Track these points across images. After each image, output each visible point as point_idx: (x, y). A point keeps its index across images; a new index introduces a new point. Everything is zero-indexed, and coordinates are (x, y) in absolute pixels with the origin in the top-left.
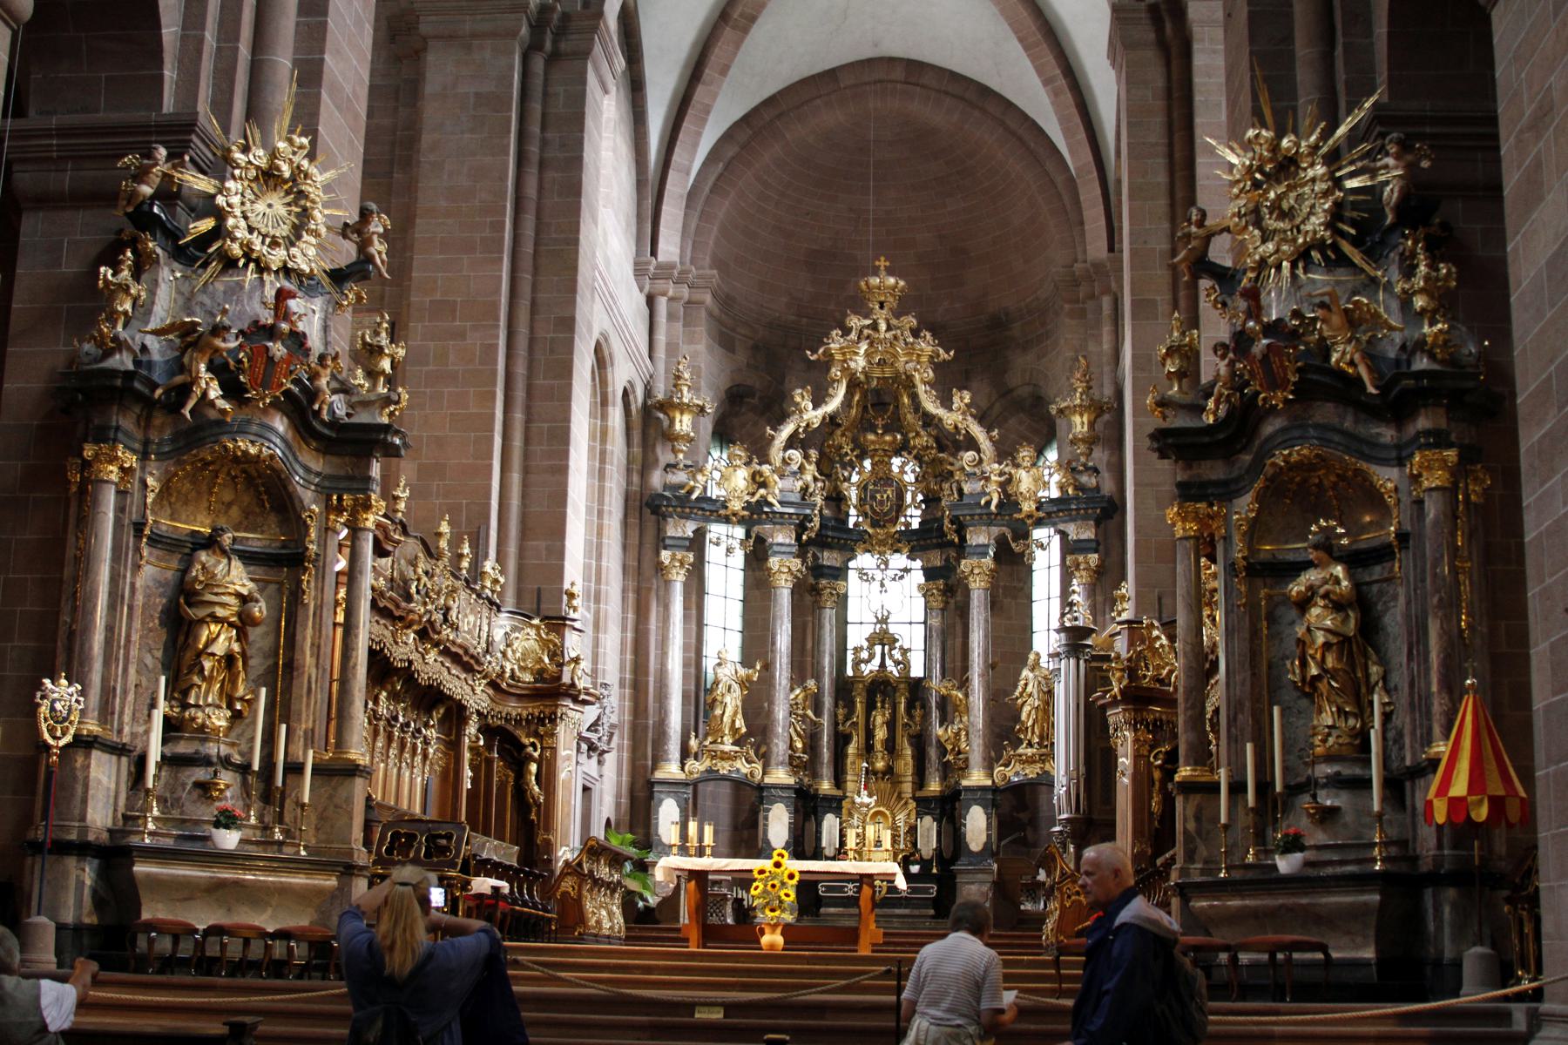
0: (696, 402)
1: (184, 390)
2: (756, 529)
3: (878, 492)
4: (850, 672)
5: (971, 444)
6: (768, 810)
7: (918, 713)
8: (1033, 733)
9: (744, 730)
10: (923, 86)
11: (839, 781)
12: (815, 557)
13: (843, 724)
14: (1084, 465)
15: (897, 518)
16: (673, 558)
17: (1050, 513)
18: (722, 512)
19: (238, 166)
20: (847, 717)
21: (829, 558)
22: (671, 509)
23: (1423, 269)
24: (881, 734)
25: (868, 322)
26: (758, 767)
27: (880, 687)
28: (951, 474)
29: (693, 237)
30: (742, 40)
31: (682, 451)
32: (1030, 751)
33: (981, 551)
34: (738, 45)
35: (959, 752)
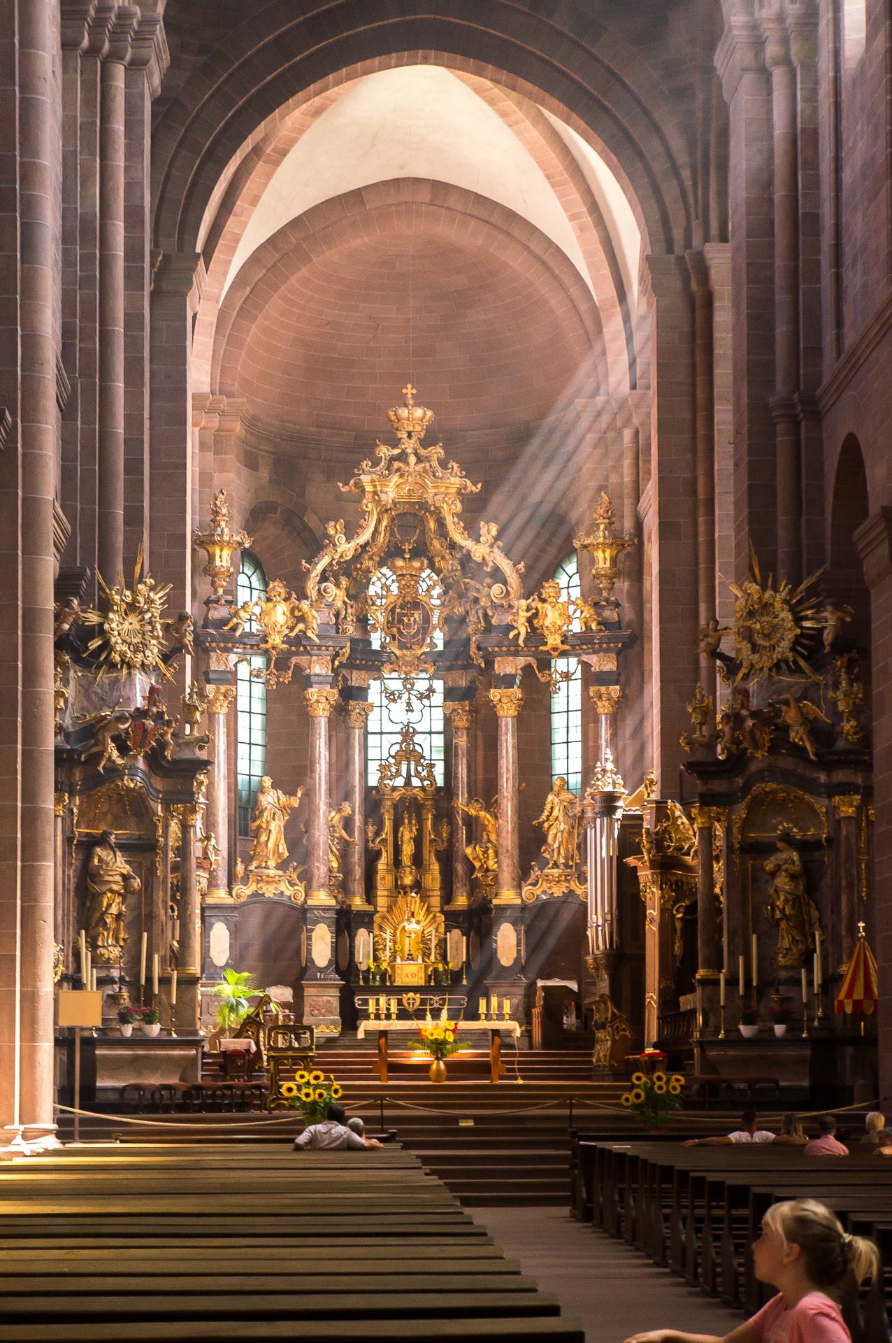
0: (235, 538)
1: (98, 756)
2: (294, 660)
3: (405, 615)
5: (497, 575)
6: (312, 930)
8: (559, 854)
9: (286, 854)
10: (448, 208)
11: (370, 896)
13: (373, 842)
14: (607, 600)
15: (424, 640)
17: (574, 645)
18: (263, 646)
19: (117, 604)
20: (377, 834)
21: (356, 679)
22: (214, 644)
23: (844, 683)
24: (408, 849)
25: (396, 452)
26: (301, 888)
27: (409, 807)
28: (476, 600)
29: (222, 364)
30: (272, 173)
31: (222, 586)
32: (556, 871)
33: (508, 681)
34: (269, 176)
35: (487, 870)
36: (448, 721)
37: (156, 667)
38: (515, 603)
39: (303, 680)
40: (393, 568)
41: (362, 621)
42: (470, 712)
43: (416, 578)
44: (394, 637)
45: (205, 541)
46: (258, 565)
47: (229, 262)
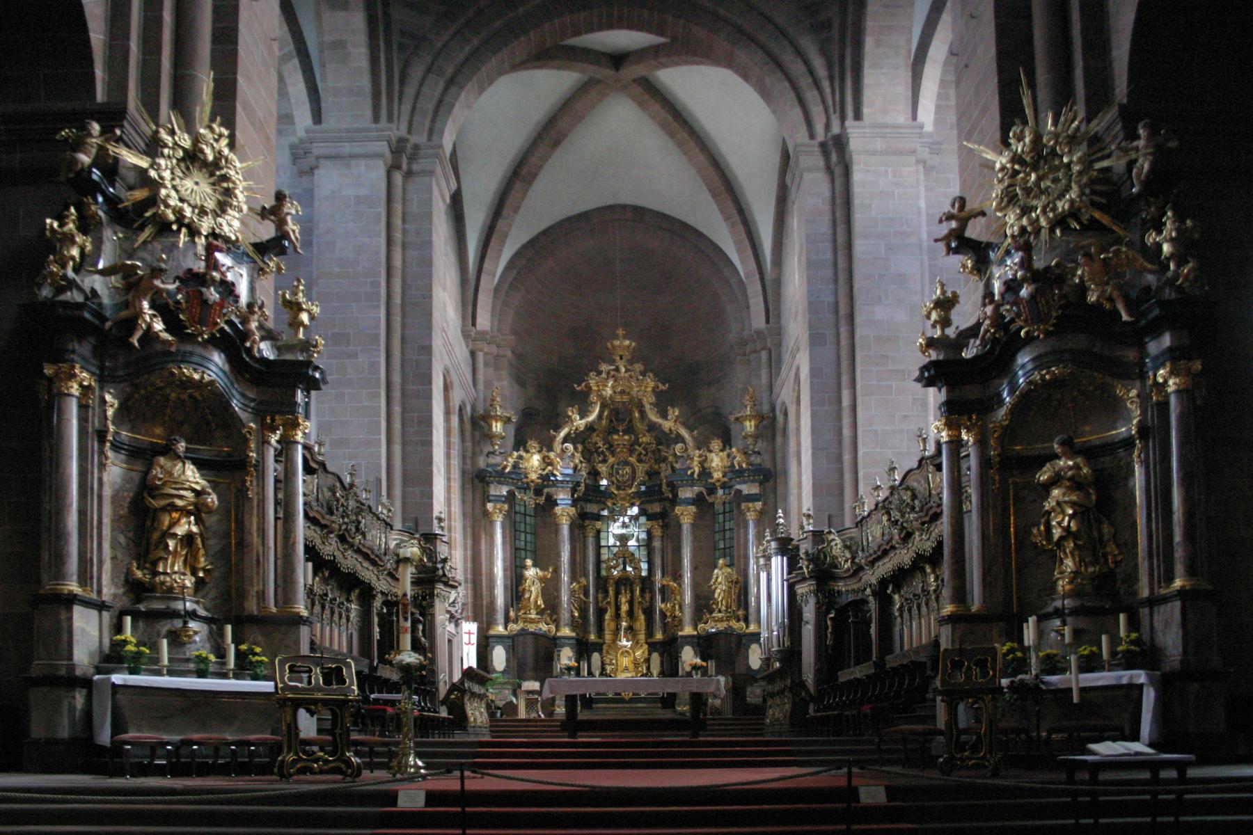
2: (546, 490)
12: (582, 508)
16: (495, 507)
18: (525, 480)
21: (592, 508)
36: (649, 533)
39: (552, 502)
42: (662, 527)
44: (613, 483)
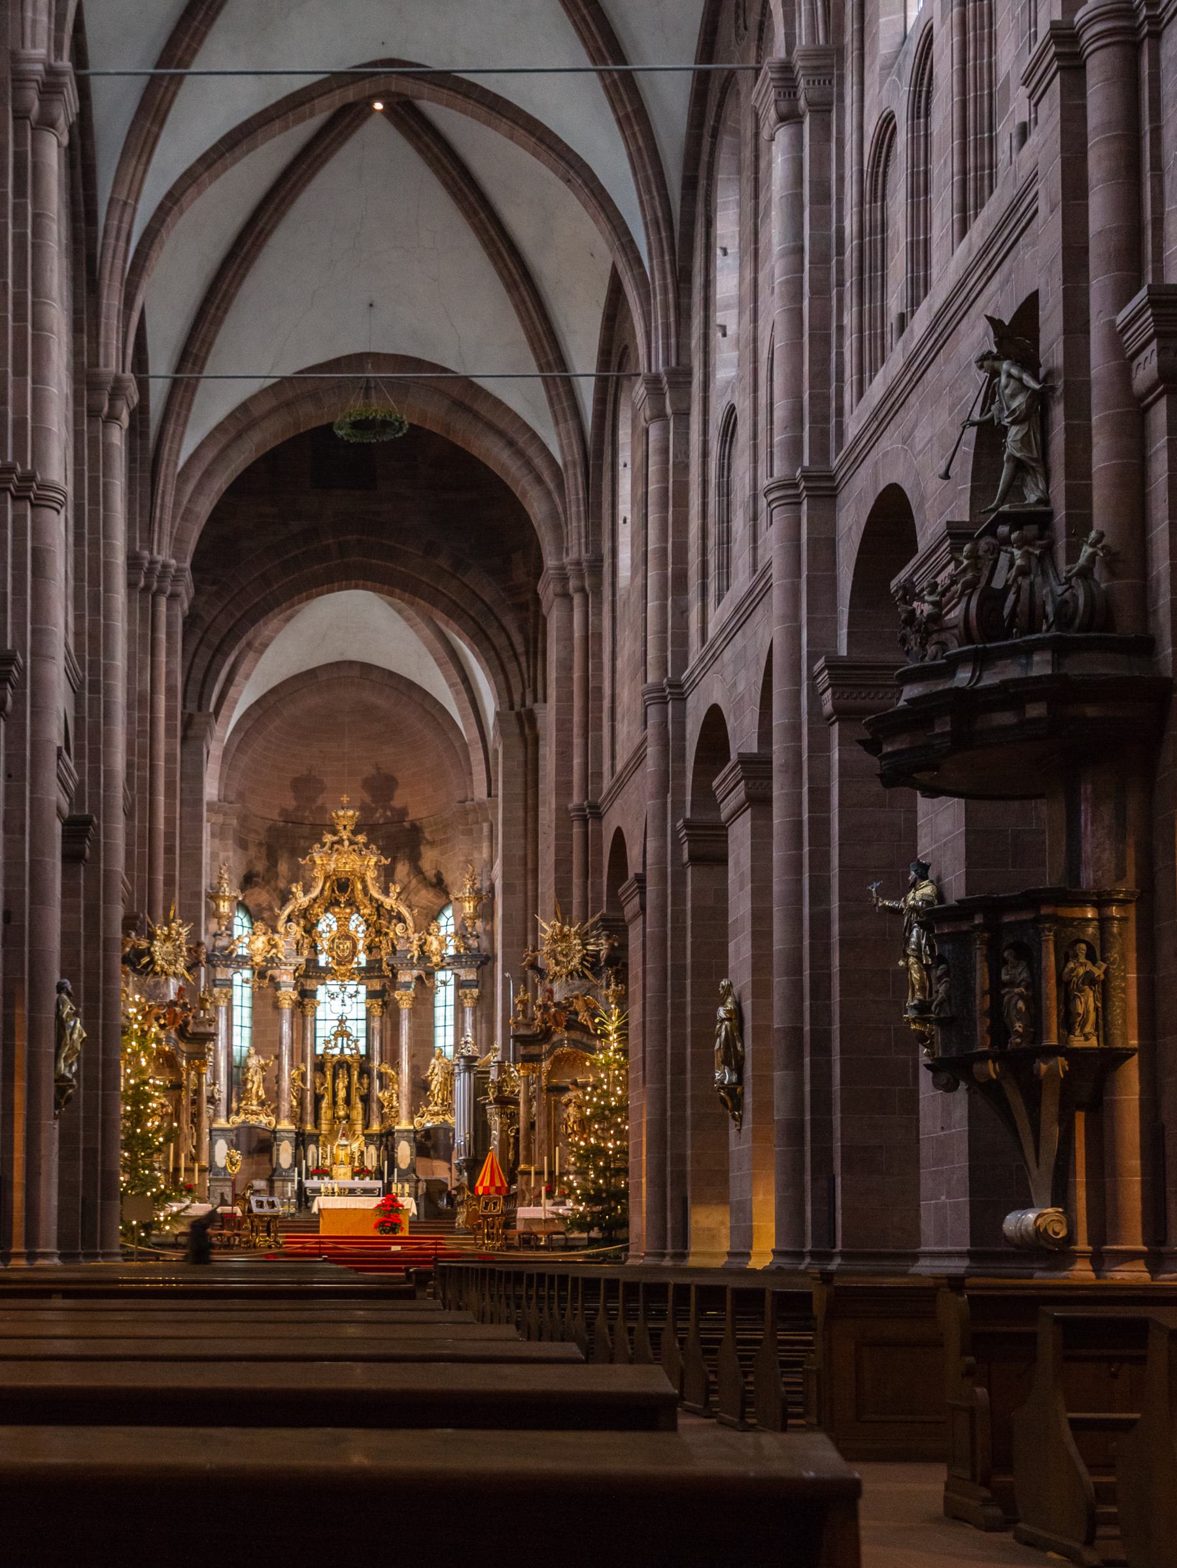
2: (269, 972)
4: (320, 1051)
5: (400, 919)
7: (365, 1081)
16: (221, 992)
20: (322, 1085)
21: (309, 985)
24: (342, 1094)
25: (335, 838)
26: (273, 1119)
27: (342, 1065)
28: (386, 934)
29: (225, 780)
32: (436, 1109)
33: (407, 986)
34: (257, 661)
36: (368, 1010)
37: (183, 975)
38: (411, 935)
40: (334, 914)
41: (314, 947)
42: (382, 1006)
43: (347, 919)
44: (333, 958)
45: (214, 896)
46: (247, 911)
47: (230, 716)
